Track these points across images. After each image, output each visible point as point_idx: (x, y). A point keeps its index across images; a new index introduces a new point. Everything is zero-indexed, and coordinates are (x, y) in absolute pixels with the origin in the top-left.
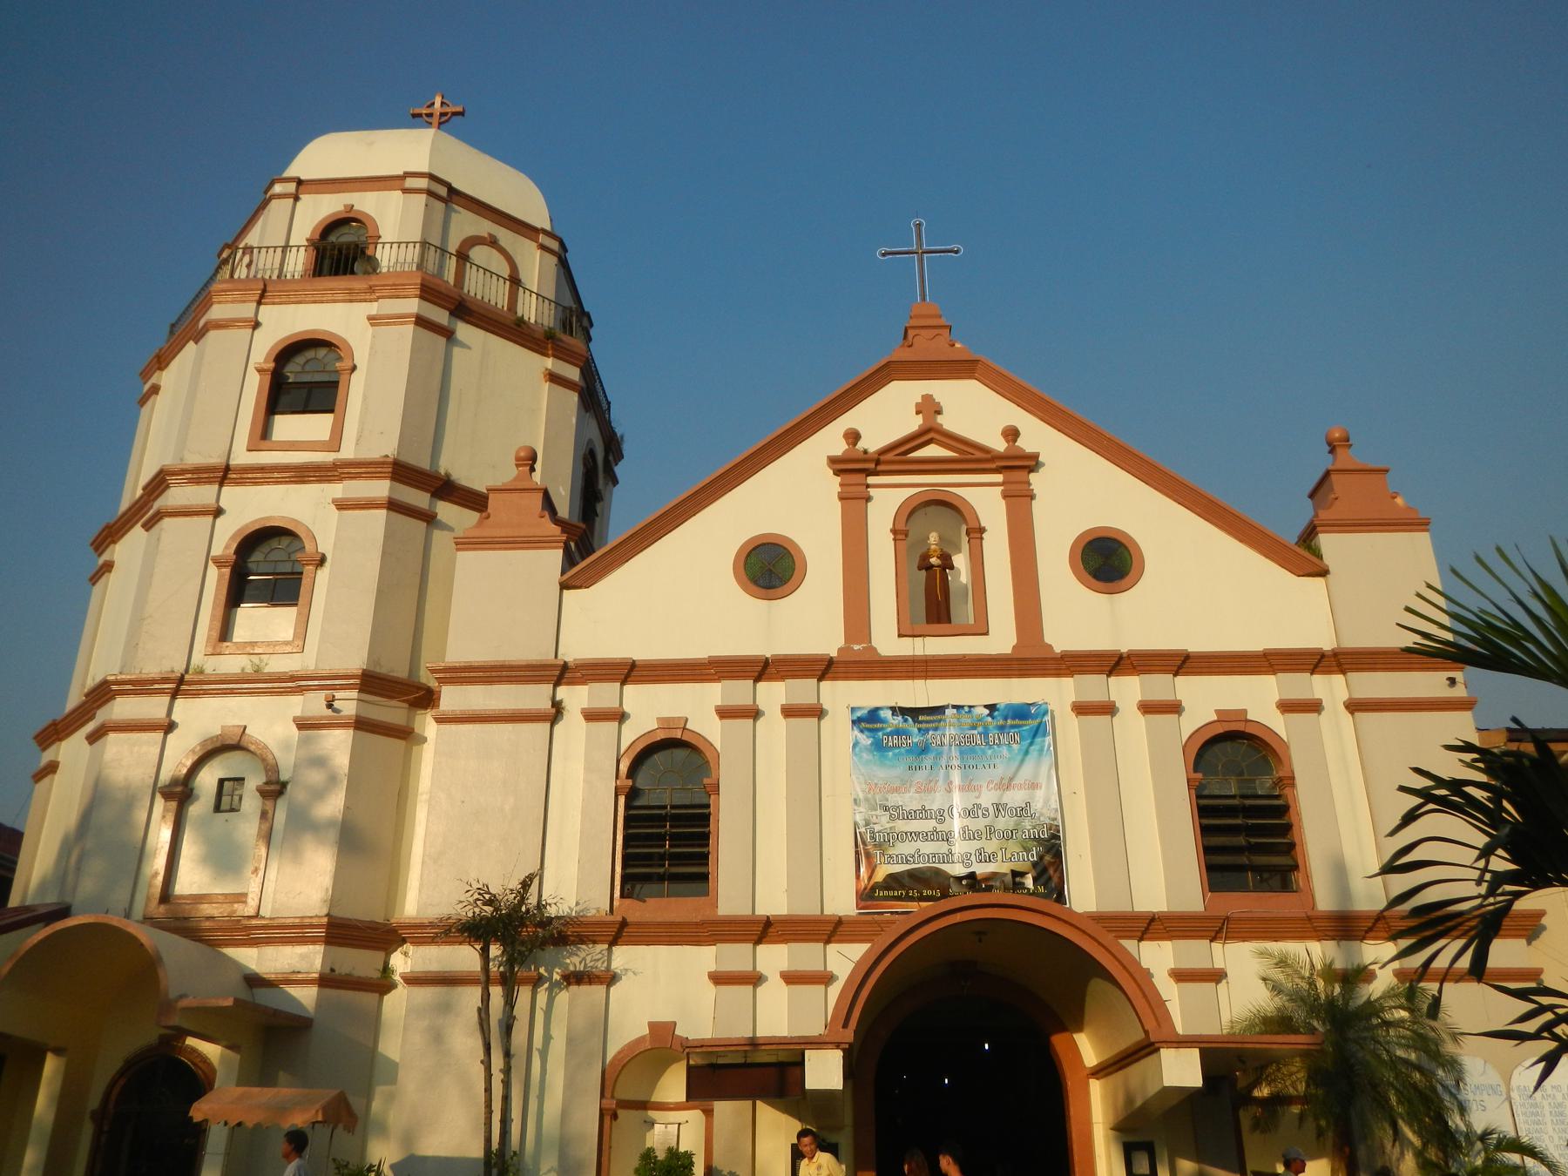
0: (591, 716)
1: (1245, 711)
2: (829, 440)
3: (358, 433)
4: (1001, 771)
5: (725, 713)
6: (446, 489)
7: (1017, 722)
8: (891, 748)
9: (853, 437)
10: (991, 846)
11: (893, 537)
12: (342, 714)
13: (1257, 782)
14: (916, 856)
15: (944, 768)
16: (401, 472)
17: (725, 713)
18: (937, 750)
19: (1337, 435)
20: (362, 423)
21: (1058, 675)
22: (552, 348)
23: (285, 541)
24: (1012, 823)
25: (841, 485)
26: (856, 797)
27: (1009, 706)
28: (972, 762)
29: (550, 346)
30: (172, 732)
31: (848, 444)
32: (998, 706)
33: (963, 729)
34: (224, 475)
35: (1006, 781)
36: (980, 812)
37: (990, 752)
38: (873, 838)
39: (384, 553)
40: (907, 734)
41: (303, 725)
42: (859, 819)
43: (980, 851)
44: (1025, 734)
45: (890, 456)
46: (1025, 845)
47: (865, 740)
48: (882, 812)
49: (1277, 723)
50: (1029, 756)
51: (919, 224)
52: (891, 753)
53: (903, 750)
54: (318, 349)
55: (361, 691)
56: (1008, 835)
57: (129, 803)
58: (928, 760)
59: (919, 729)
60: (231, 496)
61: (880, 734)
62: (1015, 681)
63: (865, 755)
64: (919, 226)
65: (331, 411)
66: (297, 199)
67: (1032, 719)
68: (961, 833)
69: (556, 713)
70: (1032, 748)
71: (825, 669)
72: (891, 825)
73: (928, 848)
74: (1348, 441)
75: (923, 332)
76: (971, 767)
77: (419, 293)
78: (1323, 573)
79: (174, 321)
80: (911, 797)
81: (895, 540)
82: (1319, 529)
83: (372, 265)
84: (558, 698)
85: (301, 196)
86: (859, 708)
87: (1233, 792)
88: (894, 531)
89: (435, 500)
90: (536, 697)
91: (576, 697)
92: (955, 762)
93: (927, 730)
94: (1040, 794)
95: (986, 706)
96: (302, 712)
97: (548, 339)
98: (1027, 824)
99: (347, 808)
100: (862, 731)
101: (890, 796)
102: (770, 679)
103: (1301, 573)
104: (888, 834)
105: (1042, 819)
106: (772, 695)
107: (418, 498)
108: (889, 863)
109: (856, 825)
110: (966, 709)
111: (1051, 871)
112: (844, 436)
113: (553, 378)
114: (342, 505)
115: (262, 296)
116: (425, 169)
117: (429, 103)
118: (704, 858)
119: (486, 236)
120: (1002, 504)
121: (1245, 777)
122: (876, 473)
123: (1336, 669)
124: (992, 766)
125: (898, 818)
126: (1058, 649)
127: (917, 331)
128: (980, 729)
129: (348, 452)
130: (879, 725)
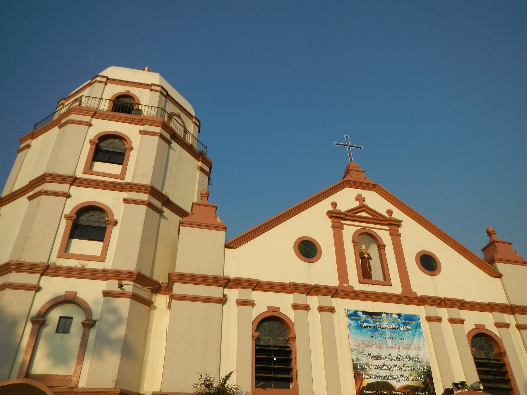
0: (240, 302)
1: (484, 326)
2: (325, 205)
3: (133, 174)
4: (406, 342)
5: (296, 307)
6: (167, 202)
7: (409, 322)
8: (365, 328)
9: (334, 205)
10: (406, 373)
11: (352, 244)
12: (125, 291)
13: (490, 354)
14: (378, 376)
15: (385, 338)
16: (154, 192)
17: (296, 307)
18: (381, 330)
19: (491, 230)
20: (135, 170)
21: (419, 305)
22: (202, 159)
24: (413, 364)
25: (332, 222)
26: (352, 348)
27: (405, 315)
28: (395, 337)
29: (201, 157)
30: (39, 292)
31: (333, 207)
32: (401, 315)
33: (389, 323)
34: (74, 181)
35: (408, 346)
36: (400, 358)
37: (401, 333)
38: (360, 366)
39: (145, 223)
40: (370, 323)
41: (107, 294)
42: (354, 357)
43: (402, 375)
44: (413, 327)
45: (350, 214)
46: (419, 374)
47: (352, 322)
48: (362, 355)
49: (496, 331)
50: (415, 336)
51: (347, 136)
52: (364, 330)
53: (368, 329)
54: (115, 139)
55: (135, 281)
56: (413, 369)
57: (14, 323)
58: (378, 334)
59: (373, 321)
61: (359, 321)
62: (403, 305)
63: (354, 330)
64: (347, 137)
65: (121, 164)
66: (106, 84)
67: (414, 321)
68: (394, 367)
69: (223, 300)
70: (416, 333)
71: (335, 292)
72: (366, 361)
73: (383, 372)
74: (494, 232)
75: (356, 172)
76: (395, 339)
77: (161, 125)
78: (500, 276)
79: (37, 122)
80: (373, 350)
81: (354, 245)
82: (496, 261)
83: (139, 112)
84: (224, 294)
85: (107, 84)
86: (350, 310)
87: (483, 357)
88: (353, 242)
89: (162, 206)
90: (216, 292)
91: (233, 294)
92: (389, 336)
93: (376, 322)
94: (421, 352)
95: (397, 314)
96: (106, 288)
97: (201, 155)
98: (418, 365)
99: (126, 335)
100: (352, 320)
101: (365, 349)
102: (312, 295)
103: (493, 276)
104: (366, 365)
105: (424, 363)
106: (313, 301)
107: (158, 204)
108: (368, 378)
109: (353, 361)
110: (389, 314)
111: (430, 386)
112: (331, 204)
113: (201, 169)
115: (94, 115)
116: (158, 84)
117: (143, 69)
118: (289, 371)
119: (177, 113)
120: (390, 238)
121: (487, 352)
122: (344, 220)
123: (511, 312)
124: (403, 339)
125: (369, 358)
126: (419, 294)
127: (353, 172)
128: (396, 323)
130: (358, 318)
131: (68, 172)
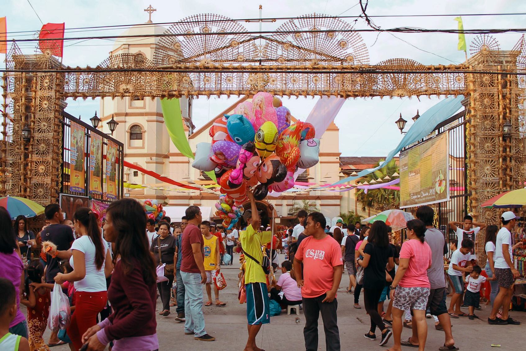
23: (138, 127)
34: (127, 115)
60: (128, 118)
114: (148, 121)
129: (147, 110)
131: (124, 111)
